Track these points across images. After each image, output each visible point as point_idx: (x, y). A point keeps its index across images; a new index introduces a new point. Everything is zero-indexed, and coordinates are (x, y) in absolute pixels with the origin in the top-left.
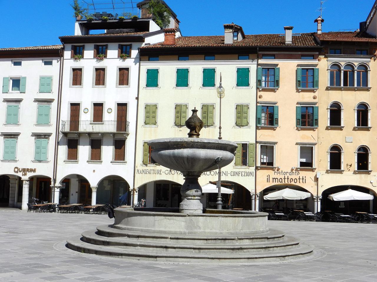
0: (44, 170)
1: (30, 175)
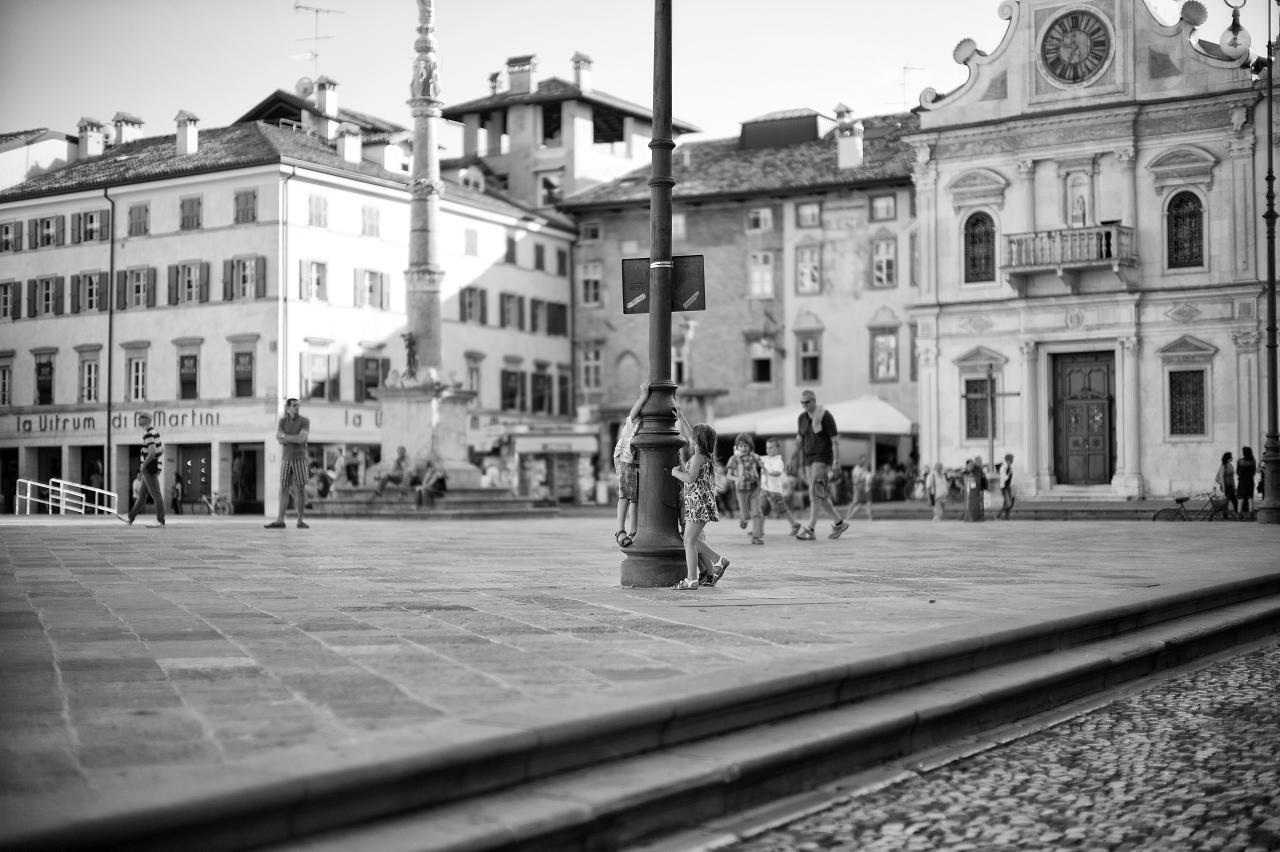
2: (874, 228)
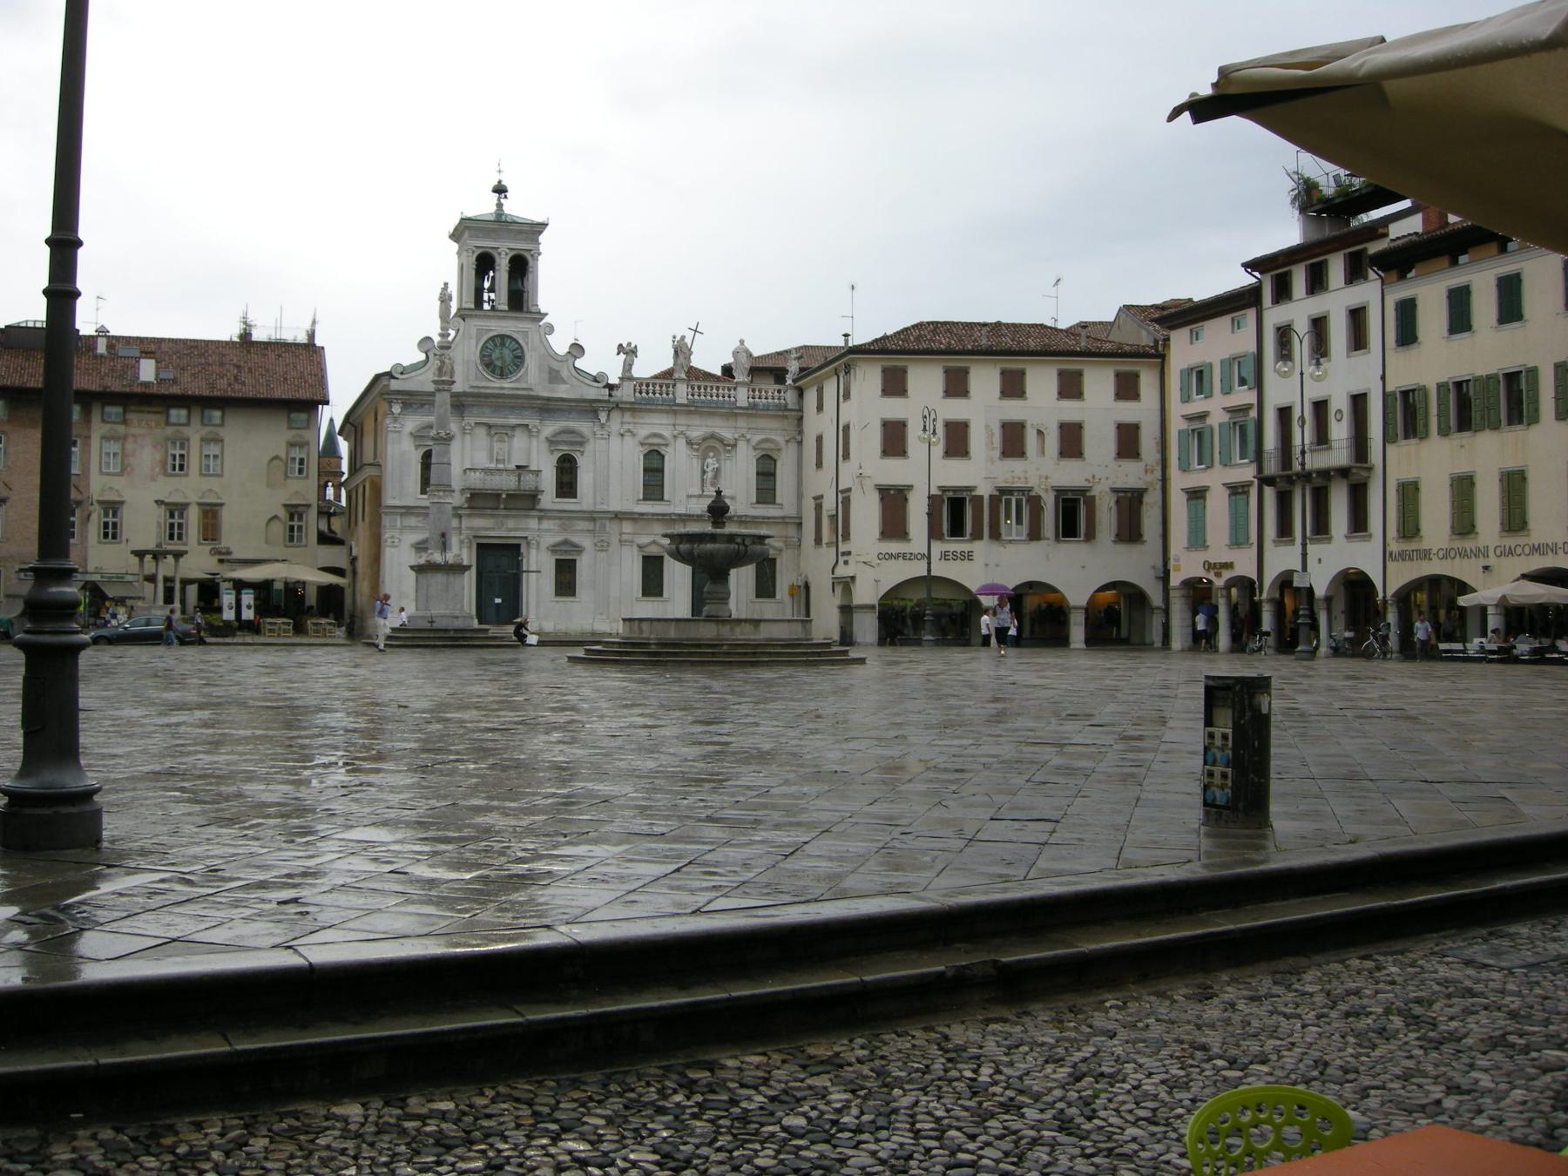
0: (1245, 565)
1: (1227, 575)
2: (170, 430)
